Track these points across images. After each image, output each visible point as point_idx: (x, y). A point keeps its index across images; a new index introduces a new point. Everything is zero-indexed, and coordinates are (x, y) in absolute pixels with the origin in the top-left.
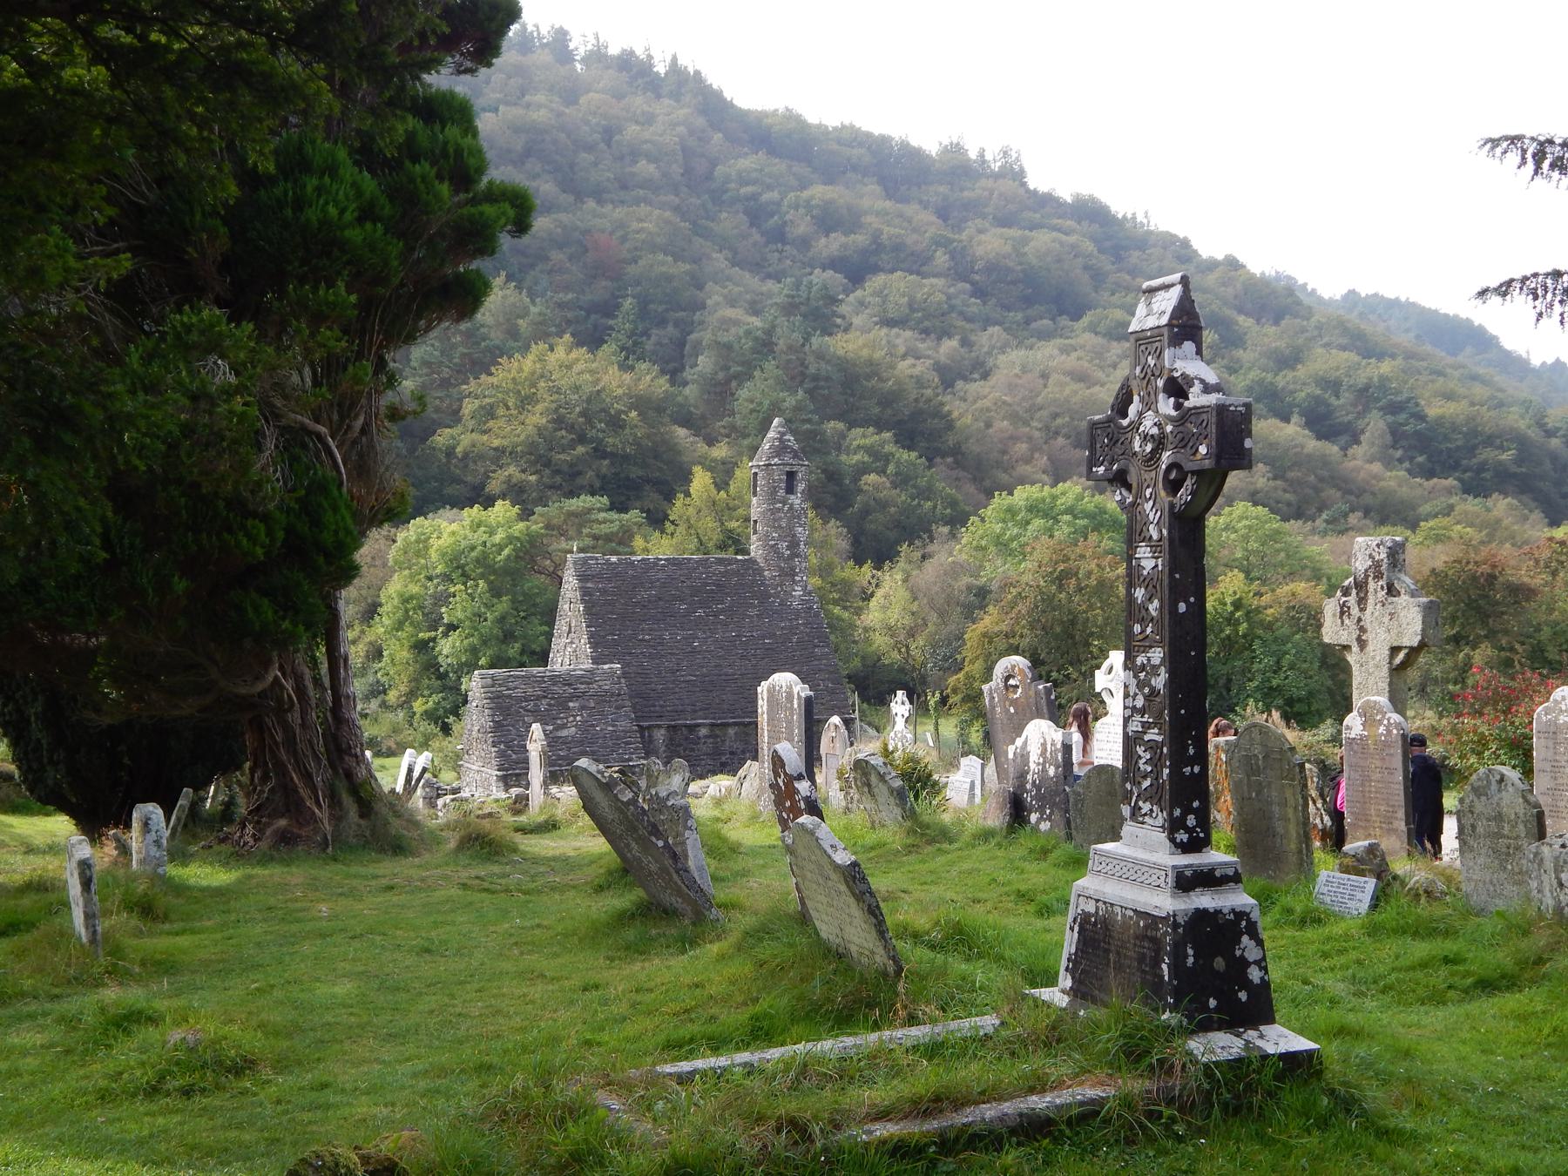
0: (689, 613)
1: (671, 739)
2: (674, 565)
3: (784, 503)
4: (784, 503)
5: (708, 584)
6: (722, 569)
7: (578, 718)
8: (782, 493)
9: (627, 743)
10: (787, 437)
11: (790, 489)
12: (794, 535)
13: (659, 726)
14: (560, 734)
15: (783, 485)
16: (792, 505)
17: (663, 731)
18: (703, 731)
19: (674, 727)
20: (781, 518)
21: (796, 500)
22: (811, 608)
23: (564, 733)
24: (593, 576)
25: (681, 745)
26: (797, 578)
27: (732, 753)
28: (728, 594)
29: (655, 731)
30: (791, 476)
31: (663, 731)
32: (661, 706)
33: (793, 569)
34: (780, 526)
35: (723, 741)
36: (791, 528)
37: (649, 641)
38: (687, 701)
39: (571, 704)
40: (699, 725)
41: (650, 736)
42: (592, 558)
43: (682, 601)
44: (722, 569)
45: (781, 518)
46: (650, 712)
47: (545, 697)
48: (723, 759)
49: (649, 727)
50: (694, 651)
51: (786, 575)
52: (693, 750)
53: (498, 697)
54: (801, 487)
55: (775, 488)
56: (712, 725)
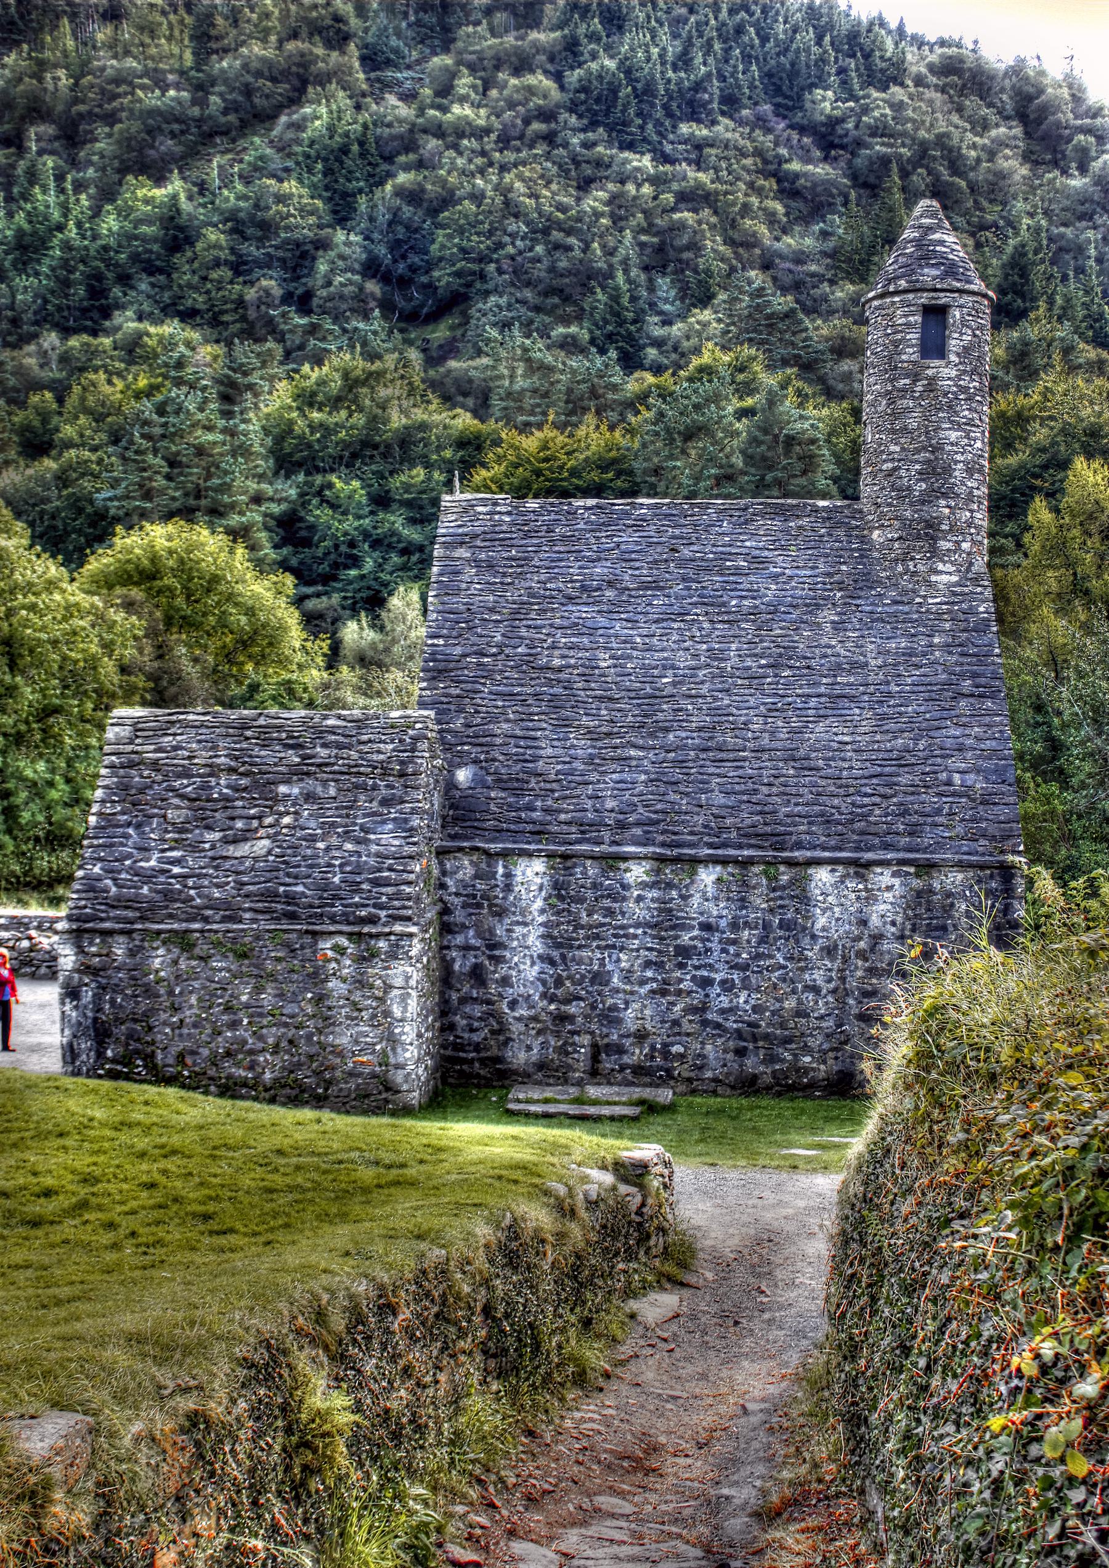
1: (557, 886)
3: (916, 377)
4: (916, 377)
7: (287, 820)
8: (910, 354)
9: (376, 882)
10: (937, 236)
11: (933, 347)
12: (937, 449)
13: (530, 855)
14: (231, 850)
15: (914, 337)
16: (932, 380)
17: (539, 865)
18: (637, 873)
19: (565, 857)
21: (946, 371)
22: (972, 612)
23: (244, 849)
24: (475, 536)
25: (581, 900)
26: (944, 545)
27: (707, 927)
29: (522, 863)
30: (936, 314)
31: (539, 865)
32: (546, 811)
34: (905, 430)
35: (684, 898)
36: (930, 430)
37: (560, 670)
38: (610, 804)
39: (283, 789)
40: (625, 858)
41: (508, 875)
46: (520, 821)
47: (232, 770)
48: (685, 938)
49: (505, 854)
51: (918, 537)
52: (610, 912)
53: (131, 765)
54: (954, 344)
55: (896, 344)
56: (661, 859)
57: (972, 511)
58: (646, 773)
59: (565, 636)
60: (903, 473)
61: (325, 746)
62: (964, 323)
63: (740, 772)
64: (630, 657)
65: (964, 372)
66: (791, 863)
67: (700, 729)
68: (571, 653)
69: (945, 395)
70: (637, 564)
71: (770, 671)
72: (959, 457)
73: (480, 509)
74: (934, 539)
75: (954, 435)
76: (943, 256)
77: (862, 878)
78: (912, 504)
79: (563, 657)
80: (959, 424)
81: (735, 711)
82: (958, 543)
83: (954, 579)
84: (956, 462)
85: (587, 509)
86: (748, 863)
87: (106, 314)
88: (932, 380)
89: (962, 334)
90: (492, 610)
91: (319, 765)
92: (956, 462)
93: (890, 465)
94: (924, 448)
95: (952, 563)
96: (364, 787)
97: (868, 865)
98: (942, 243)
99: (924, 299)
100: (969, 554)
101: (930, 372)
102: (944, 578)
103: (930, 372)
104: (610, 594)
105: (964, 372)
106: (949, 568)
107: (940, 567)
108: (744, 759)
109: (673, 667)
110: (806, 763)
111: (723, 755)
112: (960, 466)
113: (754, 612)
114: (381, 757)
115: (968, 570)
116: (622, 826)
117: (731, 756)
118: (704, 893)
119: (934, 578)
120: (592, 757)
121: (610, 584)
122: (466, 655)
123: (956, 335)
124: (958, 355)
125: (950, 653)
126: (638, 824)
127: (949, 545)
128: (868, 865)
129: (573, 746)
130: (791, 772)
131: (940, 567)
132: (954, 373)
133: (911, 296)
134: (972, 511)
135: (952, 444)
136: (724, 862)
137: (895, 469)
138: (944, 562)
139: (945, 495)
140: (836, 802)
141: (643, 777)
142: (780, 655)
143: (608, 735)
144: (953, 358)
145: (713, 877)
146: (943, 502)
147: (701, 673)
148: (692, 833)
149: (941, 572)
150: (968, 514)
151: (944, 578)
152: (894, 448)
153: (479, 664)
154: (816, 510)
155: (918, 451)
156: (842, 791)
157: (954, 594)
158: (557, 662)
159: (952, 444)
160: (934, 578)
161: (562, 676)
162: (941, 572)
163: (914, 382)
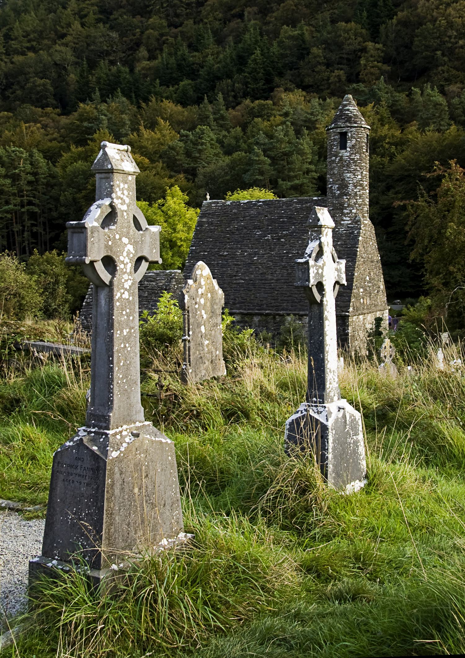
0: (261, 236)
2: (267, 205)
4: (336, 156)
5: (282, 217)
6: (299, 206)
12: (343, 180)
16: (342, 157)
20: (334, 167)
22: (353, 233)
24: (209, 214)
26: (345, 211)
28: (294, 224)
33: (342, 205)
36: (341, 174)
42: (214, 203)
43: (259, 228)
44: (299, 206)
45: (334, 167)
50: (252, 263)
51: (337, 209)
54: (349, 144)
55: (332, 145)
57: (356, 199)
58: (244, 287)
59: (230, 245)
60: (333, 188)
61: (147, 281)
62: (352, 137)
63: (270, 287)
64: (246, 251)
65: (352, 154)
66: (280, 315)
67: (261, 274)
68: (230, 250)
69: (345, 162)
70: (254, 221)
71: (286, 254)
72: (351, 182)
73: (213, 205)
74: (343, 209)
75: (348, 175)
76: (347, 115)
77: (300, 319)
78: (336, 198)
79: (227, 252)
80: (350, 171)
81: (272, 267)
82: (351, 210)
83: (350, 222)
84: (350, 184)
85: (244, 203)
86: (267, 315)
87: (272, 90)
88: (342, 157)
89: (351, 141)
90: (210, 238)
91: (145, 287)
92: (350, 184)
93: (330, 186)
94: (339, 180)
95: (349, 217)
96: (154, 293)
97: (302, 316)
98: (348, 110)
99: (339, 130)
100: (355, 214)
101: (340, 155)
102: (346, 222)
103: (340, 155)
104: (245, 231)
105: (352, 154)
106: (348, 219)
107: (344, 218)
108: (272, 283)
109: (258, 254)
110: (291, 284)
111: (267, 282)
112: (351, 185)
113: (286, 235)
114: (161, 284)
115: (355, 219)
116: (234, 304)
117: (269, 282)
118: (255, 324)
119: (342, 222)
120: (229, 283)
121: (245, 228)
122: (200, 252)
123: (349, 142)
124: (350, 148)
125: (342, 247)
126: (238, 303)
127: (348, 211)
128: (302, 316)
129: (225, 280)
130: (285, 287)
131: (344, 218)
132: (348, 154)
133: (335, 130)
134: (356, 199)
135: (348, 178)
136: (261, 315)
137: (332, 187)
138: (346, 217)
139: (346, 195)
140: (296, 296)
141: (243, 289)
142: (290, 249)
143: (235, 276)
144: (348, 149)
145: (258, 319)
146: (345, 197)
147: (265, 256)
148: (253, 306)
149: (345, 220)
150: (355, 201)
151: (346, 222)
152: (331, 180)
153: (204, 255)
154: (313, 200)
155: (337, 181)
156: (299, 293)
157: (349, 227)
158: (226, 253)
159: (348, 178)
160: (342, 222)
161: (226, 258)
162: (345, 220)
163: (336, 158)
